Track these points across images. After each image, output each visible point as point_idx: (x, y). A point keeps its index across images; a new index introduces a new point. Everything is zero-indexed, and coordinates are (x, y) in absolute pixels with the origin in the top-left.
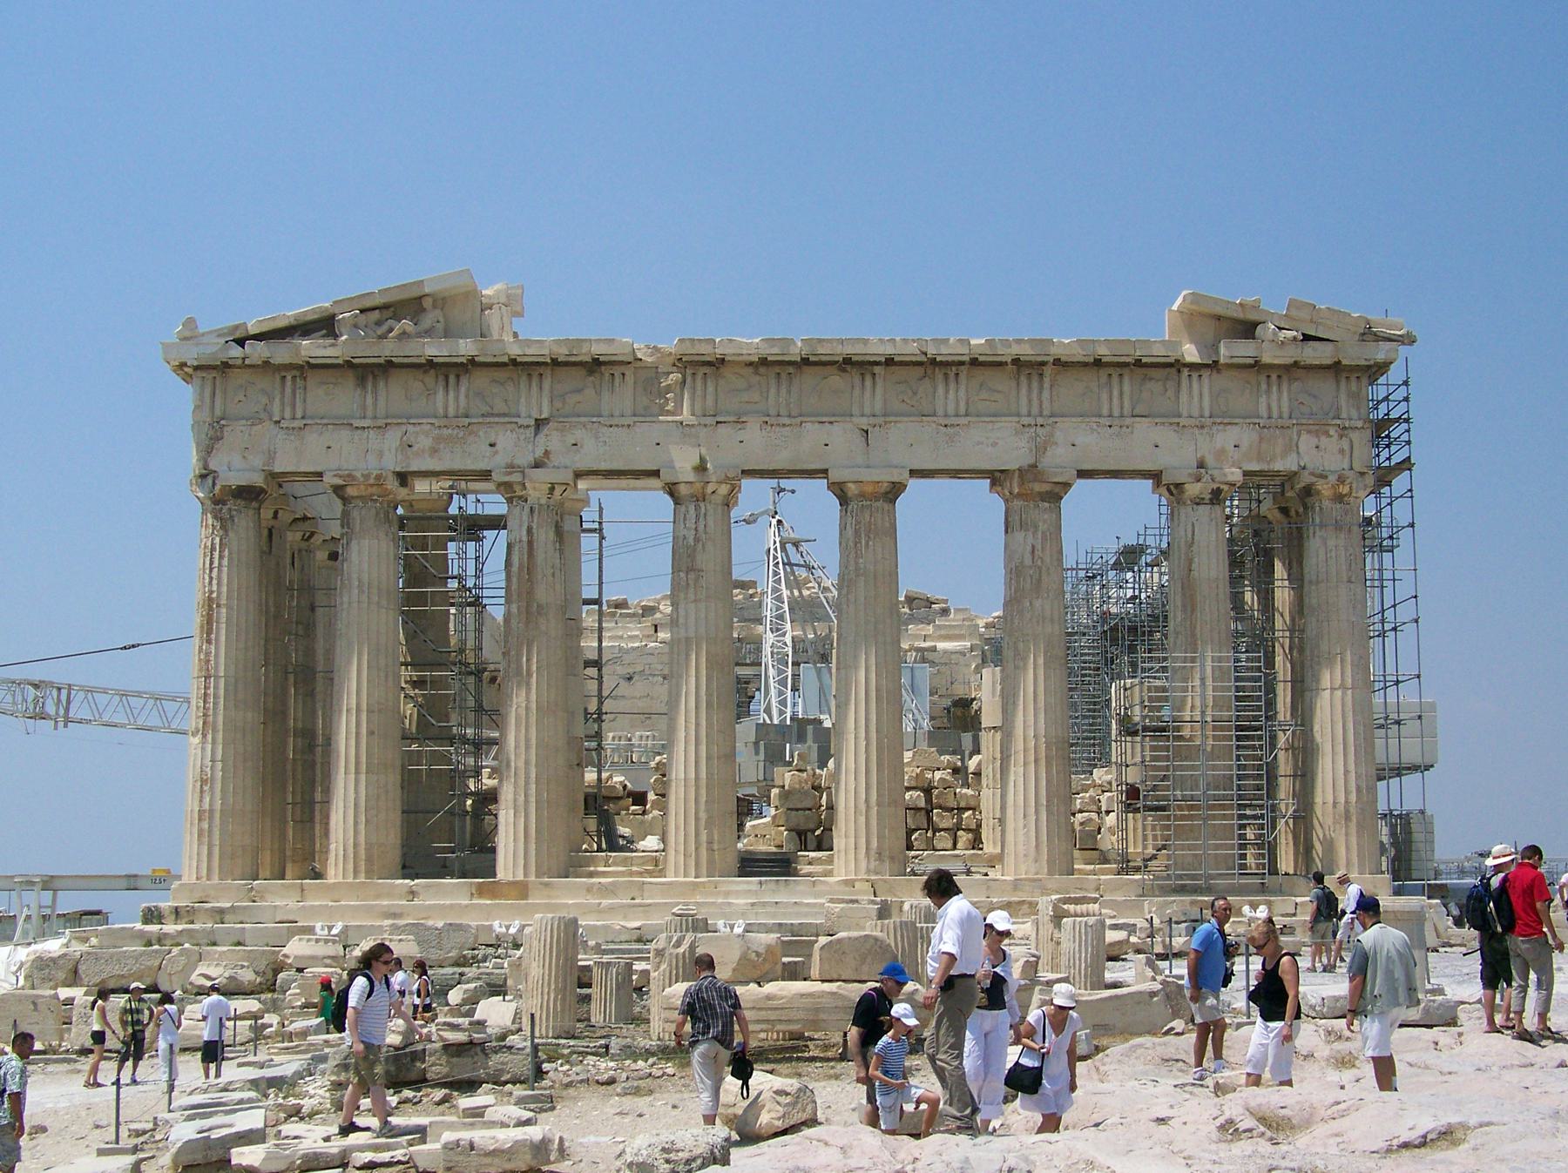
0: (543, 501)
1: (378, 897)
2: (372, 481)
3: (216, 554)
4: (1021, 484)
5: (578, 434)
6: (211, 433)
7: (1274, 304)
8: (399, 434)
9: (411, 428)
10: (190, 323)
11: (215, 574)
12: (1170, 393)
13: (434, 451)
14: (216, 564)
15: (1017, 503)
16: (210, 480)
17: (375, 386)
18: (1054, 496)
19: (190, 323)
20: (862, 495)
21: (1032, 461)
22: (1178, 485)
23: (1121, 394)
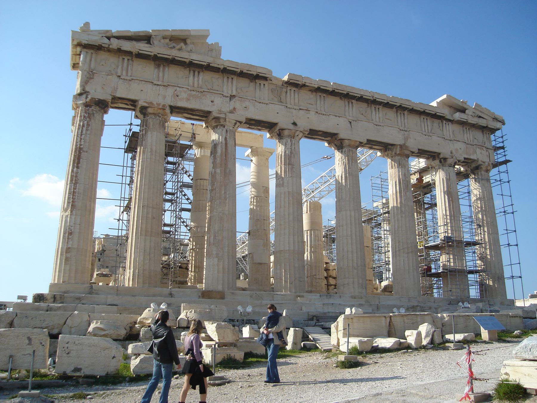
0: (231, 128)
2: (161, 107)
3: (85, 129)
4: (400, 151)
5: (247, 103)
6: (88, 75)
8: (173, 90)
9: (178, 89)
10: (87, 24)
11: (82, 137)
12: (441, 128)
13: (188, 100)
14: (84, 132)
16: (84, 96)
17: (164, 70)
18: (408, 157)
19: (87, 24)
20: (349, 146)
21: (404, 142)
22: (445, 159)
23: (427, 126)
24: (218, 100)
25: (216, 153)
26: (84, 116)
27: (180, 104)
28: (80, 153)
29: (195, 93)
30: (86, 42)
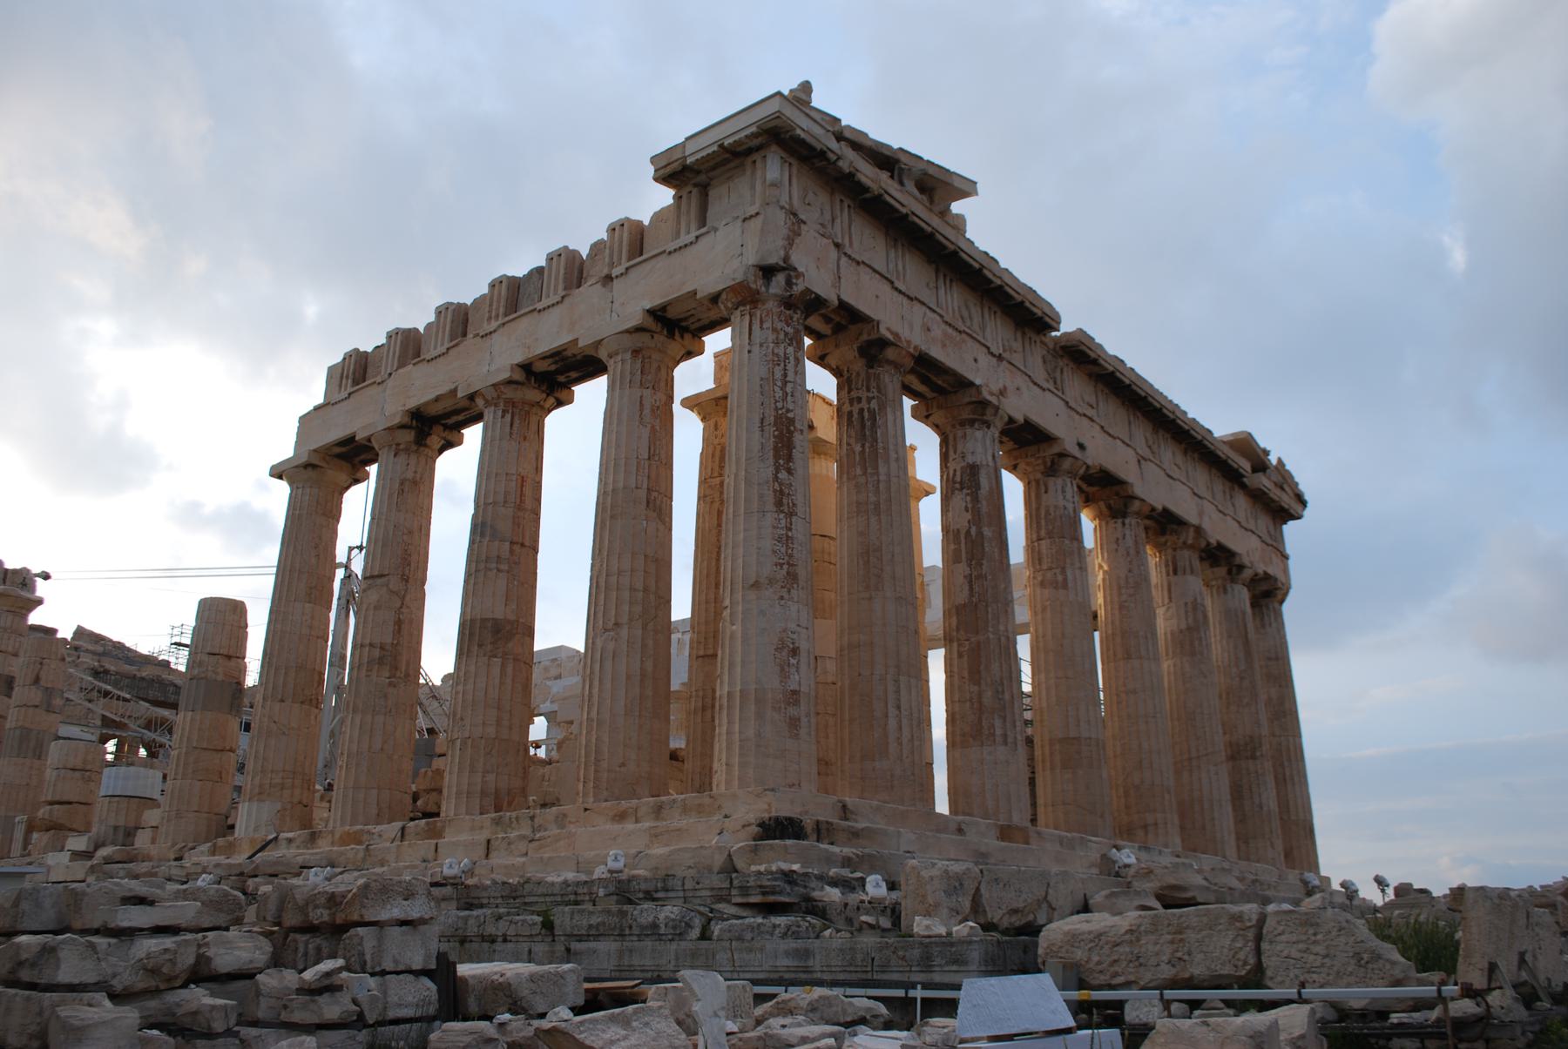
1: (938, 831)
3: (790, 367)
5: (1020, 380)
7: (1273, 459)
10: (806, 87)
11: (789, 389)
13: (944, 346)
15: (1186, 553)
16: (780, 278)
19: (806, 87)
20: (1138, 514)
22: (1241, 567)
24: (985, 360)
25: (978, 487)
26: (786, 334)
27: (936, 353)
28: (791, 433)
29: (950, 331)
30: (803, 135)
